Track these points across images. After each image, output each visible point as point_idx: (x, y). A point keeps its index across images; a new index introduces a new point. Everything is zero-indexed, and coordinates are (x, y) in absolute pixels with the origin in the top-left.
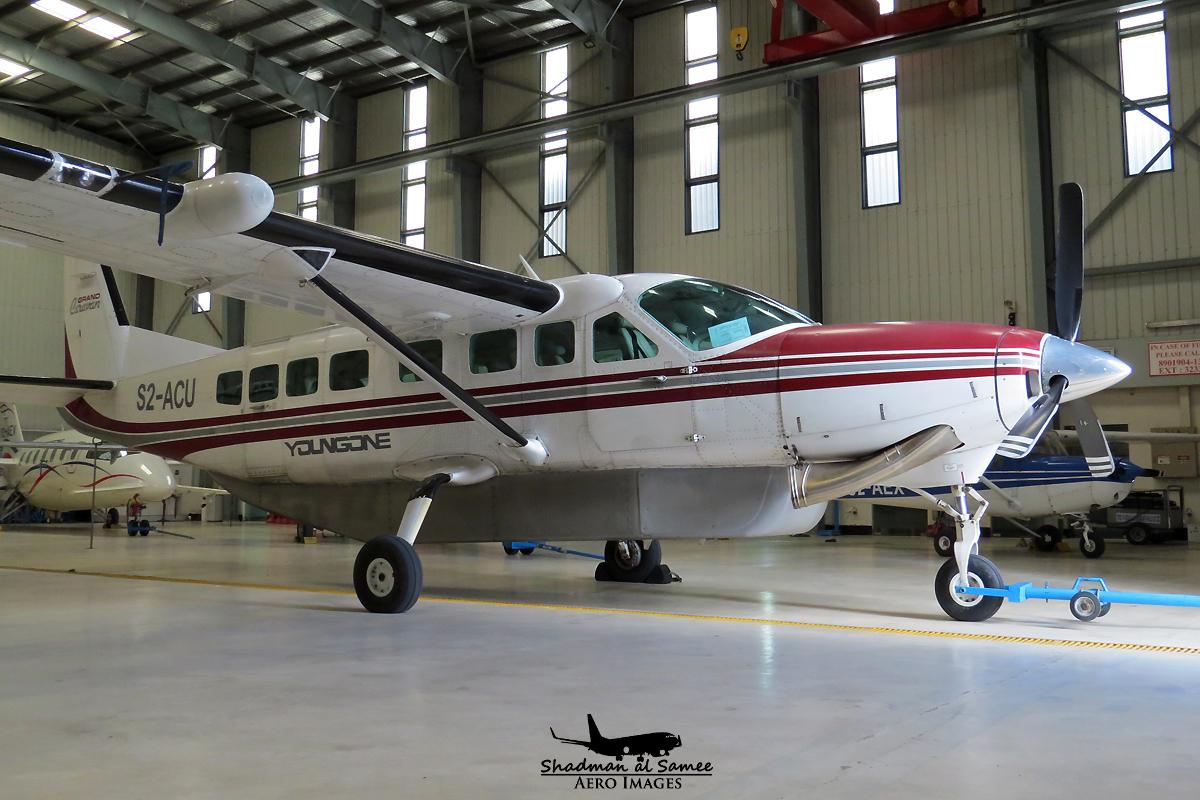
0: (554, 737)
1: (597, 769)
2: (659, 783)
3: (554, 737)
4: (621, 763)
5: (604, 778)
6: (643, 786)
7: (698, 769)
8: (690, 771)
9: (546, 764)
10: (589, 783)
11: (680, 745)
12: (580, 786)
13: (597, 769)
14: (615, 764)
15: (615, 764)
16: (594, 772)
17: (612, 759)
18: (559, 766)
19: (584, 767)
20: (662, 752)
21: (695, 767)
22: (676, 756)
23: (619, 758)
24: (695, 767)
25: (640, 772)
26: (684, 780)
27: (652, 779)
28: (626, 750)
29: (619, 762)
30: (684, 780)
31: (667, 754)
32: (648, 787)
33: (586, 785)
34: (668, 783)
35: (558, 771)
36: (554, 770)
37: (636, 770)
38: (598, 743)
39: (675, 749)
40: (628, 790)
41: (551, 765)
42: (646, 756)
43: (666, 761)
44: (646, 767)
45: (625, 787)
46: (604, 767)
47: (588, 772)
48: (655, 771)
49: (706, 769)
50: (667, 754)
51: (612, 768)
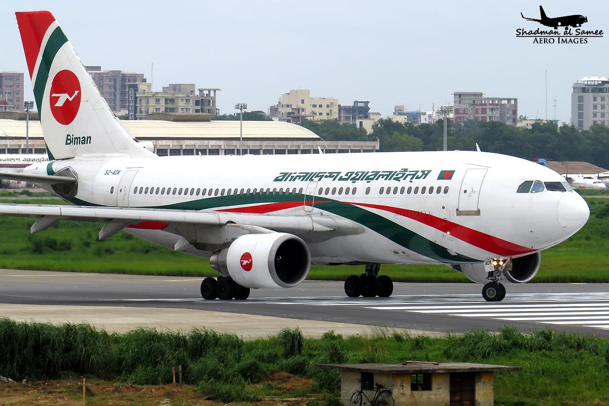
0: (523, 17)
1: (544, 34)
2: (576, 41)
3: (523, 17)
4: (557, 30)
5: (548, 38)
6: (568, 42)
7: (596, 33)
8: (592, 35)
9: (518, 31)
11: (587, 21)
12: (536, 42)
13: (544, 34)
14: (554, 31)
15: (554, 31)
16: (543, 35)
17: (552, 29)
18: (525, 32)
19: (538, 32)
20: (578, 25)
21: (594, 32)
22: (584, 27)
23: (556, 28)
24: (594, 32)
25: (566, 35)
26: (589, 39)
27: (572, 39)
28: (559, 24)
29: (556, 30)
30: (589, 39)
31: (580, 26)
32: (570, 42)
33: (539, 42)
34: (581, 41)
35: (525, 35)
36: (523, 34)
37: (564, 34)
38: (545, 20)
39: (584, 23)
40: (560, 44)
41: (521, 31)
42: (569, 27)
43: (580, 30)
44: (570, 32)
45: (559, 43)
46: (548, 32)
47: (540, 35)
48: (574, 35)
49: (600, 33)
50: (580, 26)
51: (552, 33)
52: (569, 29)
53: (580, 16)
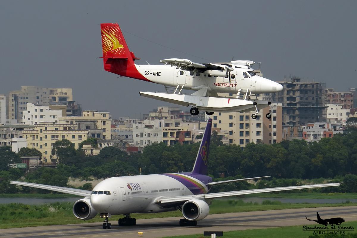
0: (307, 219)
1: (319, 229)
3: (307, 219)
4: (326, 227)
5: (322, 231)
7: (349, 228)
8: (347, 229)
10: (317, 233)
13: (319, 229)
17: (324, 226)
19: (315, 228)
20: (339, 223)
23: (326, 225)
28: (328, 223)
29: (326, 226)
31: (340, 224)
32: (335, 234)
35: (308, 229)
36: (307, 229)
37: (331, 229)
41: (306, 227)
42: (334, 224)
43: (340, 226)
44: (334, 228)
46: (322, 228)
47: (317, 229)
49: (352, 228)
50: (340, 224)
52: (334, 226)
53: (341, 218)
